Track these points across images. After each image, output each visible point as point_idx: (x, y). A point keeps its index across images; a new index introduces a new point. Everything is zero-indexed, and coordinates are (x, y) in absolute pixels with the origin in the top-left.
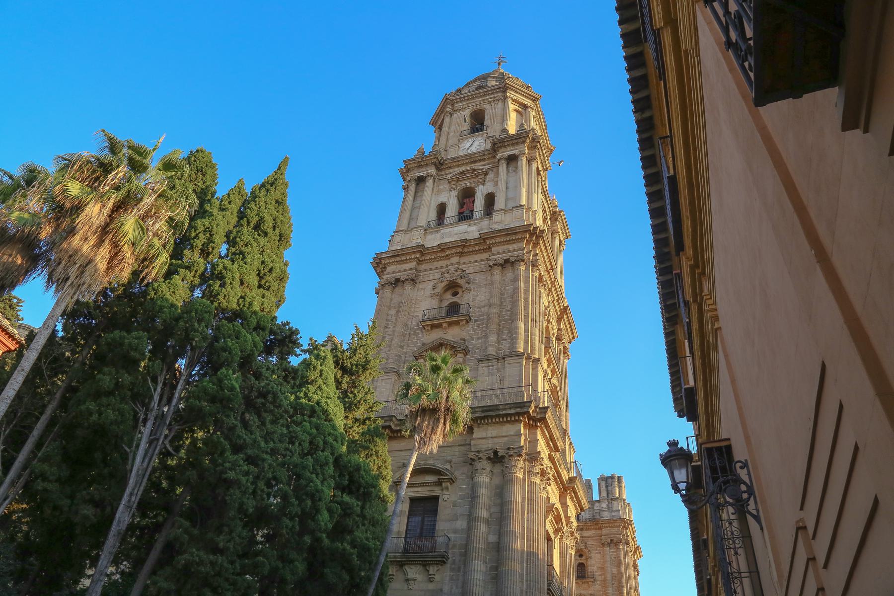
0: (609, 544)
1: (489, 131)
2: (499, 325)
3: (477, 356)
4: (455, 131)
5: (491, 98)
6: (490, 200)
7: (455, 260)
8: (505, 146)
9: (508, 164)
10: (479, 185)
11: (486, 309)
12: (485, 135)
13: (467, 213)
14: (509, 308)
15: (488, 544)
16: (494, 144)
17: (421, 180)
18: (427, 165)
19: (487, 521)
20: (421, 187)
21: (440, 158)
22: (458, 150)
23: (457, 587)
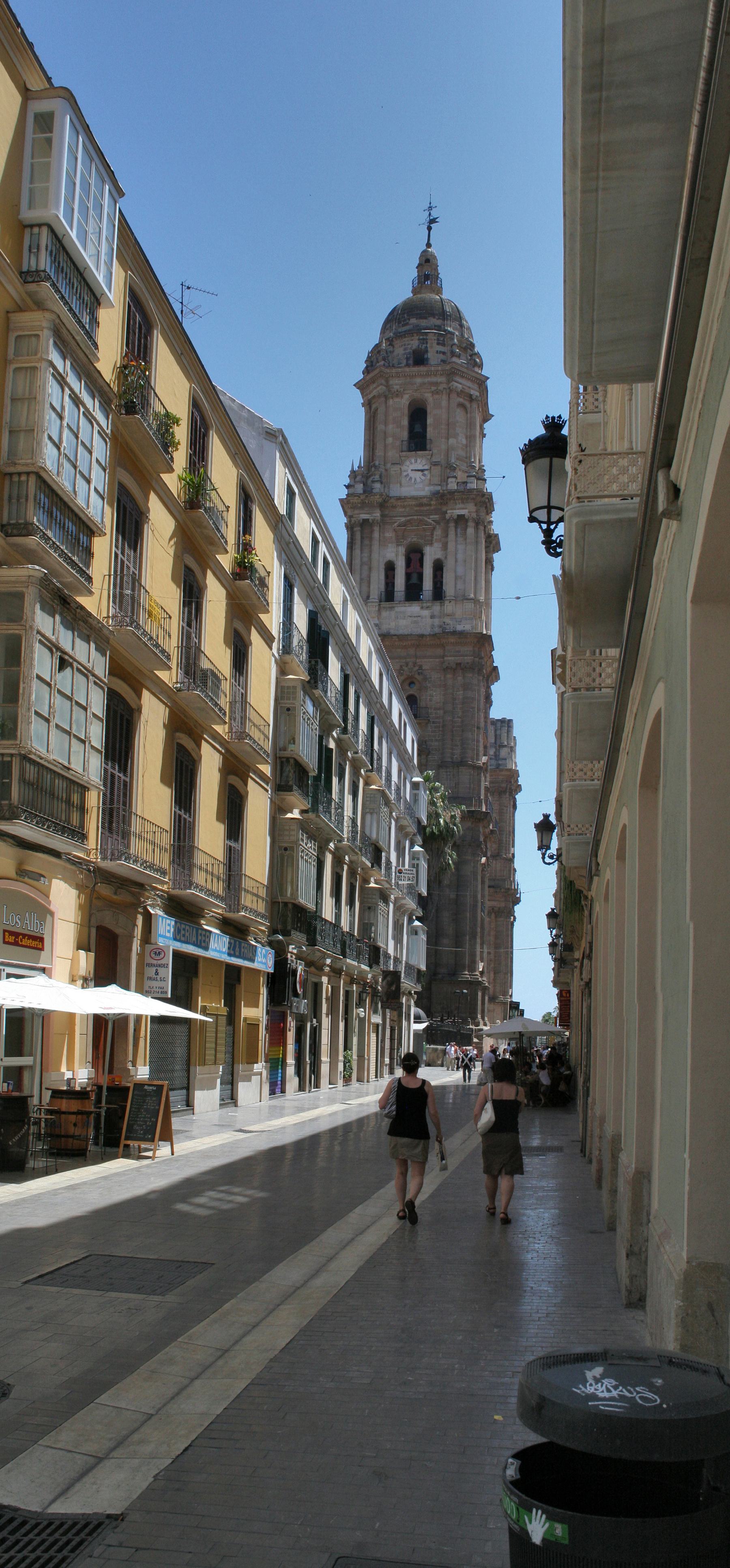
1: (435, 451)
2: (452, 731)
6: (438, 567)
7: (412, 651)
10: (426, 545)
11: (441, 712)
12: (429, 457)
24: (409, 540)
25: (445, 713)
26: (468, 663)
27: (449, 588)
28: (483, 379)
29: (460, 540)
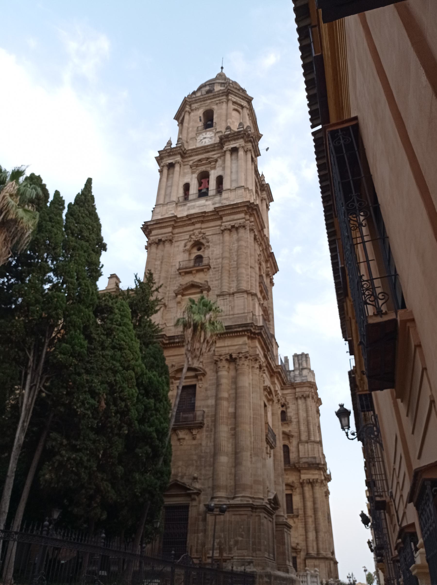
0: (301, 398)
1: (218, 127)
2: (229, 271)
3: (217, 292)
4: (193, 127)
5: (217, 100)
6: (220, 180)
7: (198, 226)
8: (229, 141)
9: (231, 154)
13: (204, 191)
14: (236, 259)
15: (229, 413)
16: (221, 139)
17: (171, 166)
18: (175, 155)
19: (227, 399)
20: (171, 171)
21: (183, 149)
22: (196, 142)
23: (211, 442)
24: (200, 170)
25: (223, 259)
26: (240, 224)
27: (226, 185)
28: (250, 98)
29: (234, 162)
